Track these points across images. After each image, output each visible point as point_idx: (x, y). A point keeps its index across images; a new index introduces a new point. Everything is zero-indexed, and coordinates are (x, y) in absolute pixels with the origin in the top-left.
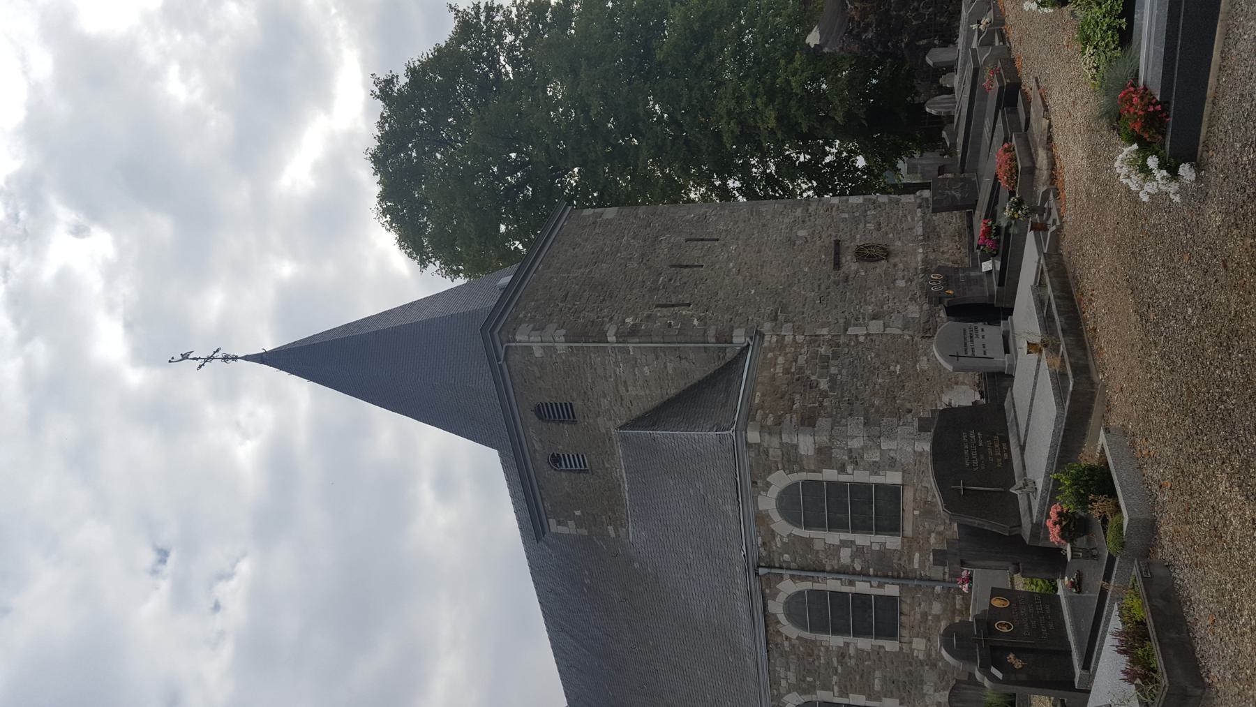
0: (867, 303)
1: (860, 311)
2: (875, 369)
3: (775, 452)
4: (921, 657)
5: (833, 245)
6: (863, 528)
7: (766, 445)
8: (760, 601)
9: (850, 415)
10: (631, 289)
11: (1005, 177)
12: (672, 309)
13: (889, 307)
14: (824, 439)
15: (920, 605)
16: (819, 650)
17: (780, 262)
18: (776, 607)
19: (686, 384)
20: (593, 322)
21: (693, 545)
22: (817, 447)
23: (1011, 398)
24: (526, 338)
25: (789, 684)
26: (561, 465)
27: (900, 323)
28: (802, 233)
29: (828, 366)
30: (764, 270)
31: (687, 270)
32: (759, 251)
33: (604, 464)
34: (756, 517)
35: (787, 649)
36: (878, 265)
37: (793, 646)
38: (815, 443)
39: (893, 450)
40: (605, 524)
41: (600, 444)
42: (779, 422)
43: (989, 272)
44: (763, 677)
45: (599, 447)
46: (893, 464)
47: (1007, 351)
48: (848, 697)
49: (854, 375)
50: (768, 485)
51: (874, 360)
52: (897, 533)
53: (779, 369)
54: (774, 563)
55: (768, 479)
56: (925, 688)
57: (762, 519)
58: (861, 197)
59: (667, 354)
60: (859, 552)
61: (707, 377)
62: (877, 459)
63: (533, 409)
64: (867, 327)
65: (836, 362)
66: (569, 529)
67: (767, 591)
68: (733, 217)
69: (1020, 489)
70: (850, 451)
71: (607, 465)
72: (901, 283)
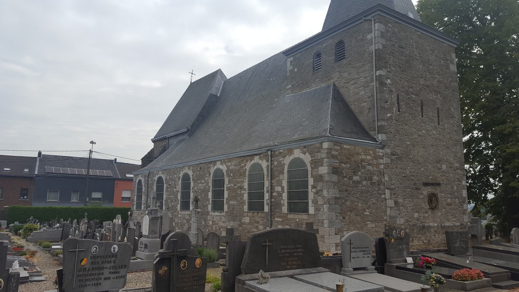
0: (404, 199)
1: (399, 195)
2: (366, 202)
3: (319, 156)
4: (243, 220)
5: (437, 182)
6: (290, 197)
7: (322, 151)
8: (258, 152)
9: (340, 191)
10: (407, 81)
11: (460, 274)
12: (396, 103)
13: (402, 209)
14: (327, 178)
15: (262, 220)
16: (242, 178)
17: (426, 156)
18: (256, 159)
19: (357, 113)
20: (387, 62)
21: (282, 122)
22: (323, 175)
23: (323, 271)
24: (377, 29)
25: (229, 166)
26: (316, 58)
27: (393, 214)
28: (444, 167)
29: (367, 180)
30: (422, 149)
31: (420, 109)
32: (432, 145)
33: (317, 79)
34: (291, 149)
35: (242, 164)
36: (426, 204)
38: (324, 174)
39: (324, 210)
40: (292, 83)
41: (326, 75)
42: (333, 157)
43: (406, 261)
44: (231, 155)
45: (325, 75)
46: (317, 210)
47: (355, 269)
48: (227, 190)
49: (362, 192)
50: (305, 154)
51: (371, 202)
52: (289, 211)
53: (363, 157)
54: (273, 158)
55: (307, 153)
56: (232, 222)
57: (290, 151)
58: (467, 196)
59: (371, 102)
60: (280, 195)
61: (360, 123)
62: (319, 203)
63: (341, 40)
64: (391, 199)
65: (369, 184)
66: (289, 67)
67: (262, 155)
68: (453, 132)
69: (262, 275)
70: (322, 191)
71: (317, 80)
72: (416, 215)
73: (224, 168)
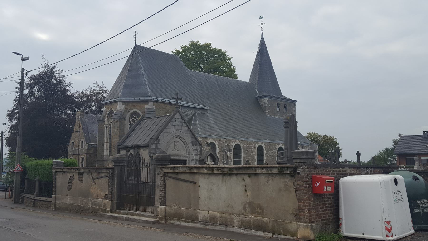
67: (299, 145)
71: (278, 115)
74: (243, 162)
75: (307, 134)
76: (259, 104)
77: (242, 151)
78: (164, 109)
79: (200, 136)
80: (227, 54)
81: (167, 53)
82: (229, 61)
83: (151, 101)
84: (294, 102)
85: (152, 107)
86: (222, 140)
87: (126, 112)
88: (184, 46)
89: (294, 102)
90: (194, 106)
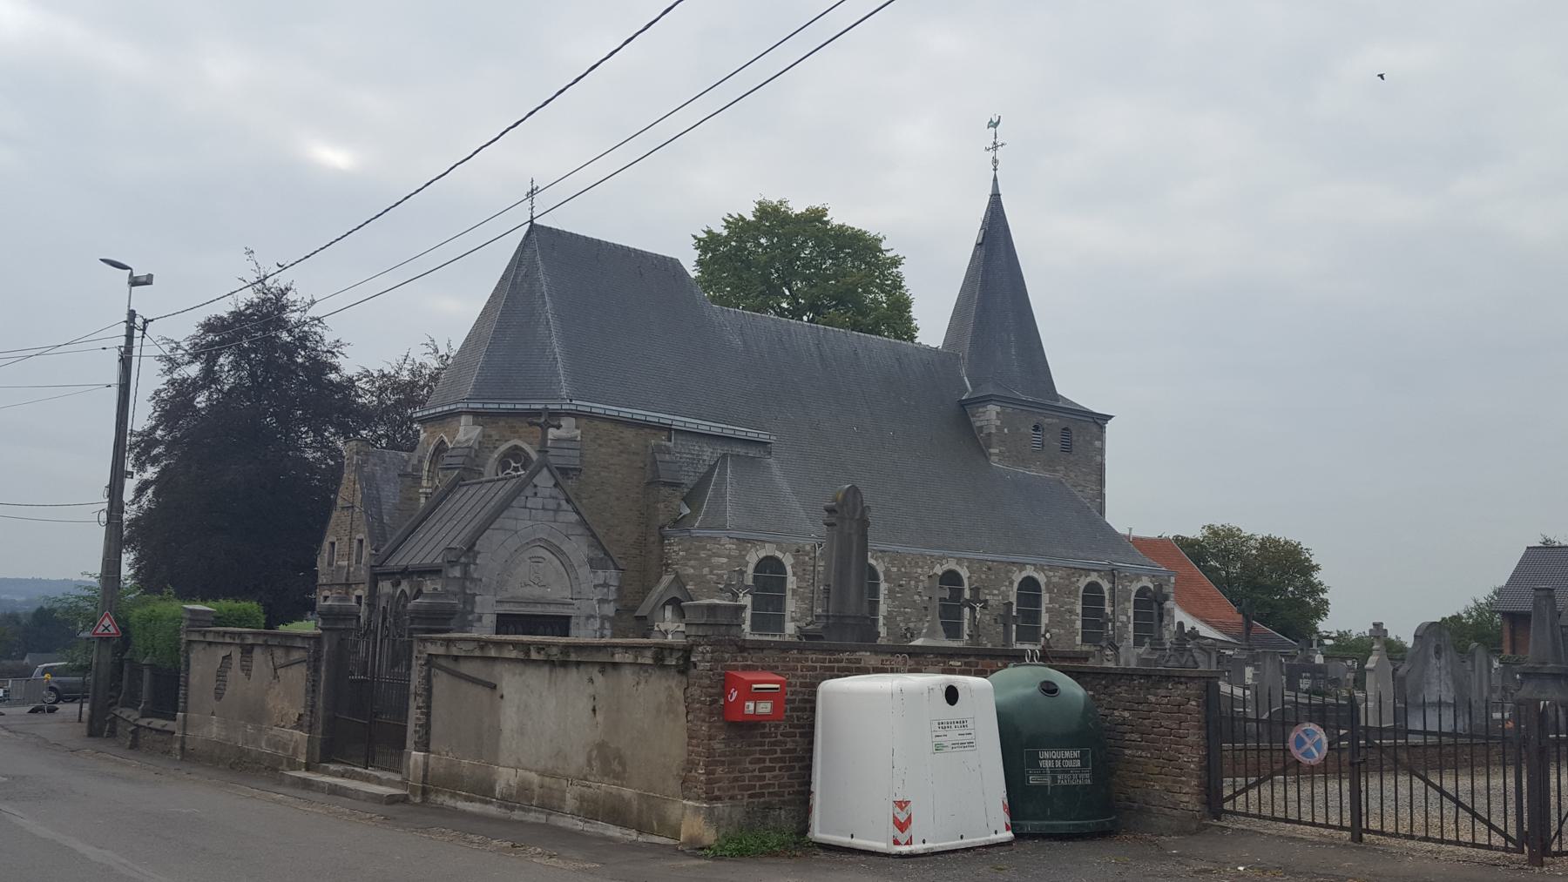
37: (1073, 583)
57: (1138, 577)
60: (1125, 625)
67: (1103, 573)
73: (1041, 578)
74: (884, 624)
75: (1204, 531)
76: (969, 425)
77: (883, 587)
78: (613, 442)
79: (730, 533)
80: (884, 246)
81: (642, 251)
82: (895, 270)
83: (569, 414)
84: (1099, 422)
85: (569, 435)
86: (808, 548)
87: (487, 448)
88: (735, 219)
89: (1099, 421)
90: (720, 430)
